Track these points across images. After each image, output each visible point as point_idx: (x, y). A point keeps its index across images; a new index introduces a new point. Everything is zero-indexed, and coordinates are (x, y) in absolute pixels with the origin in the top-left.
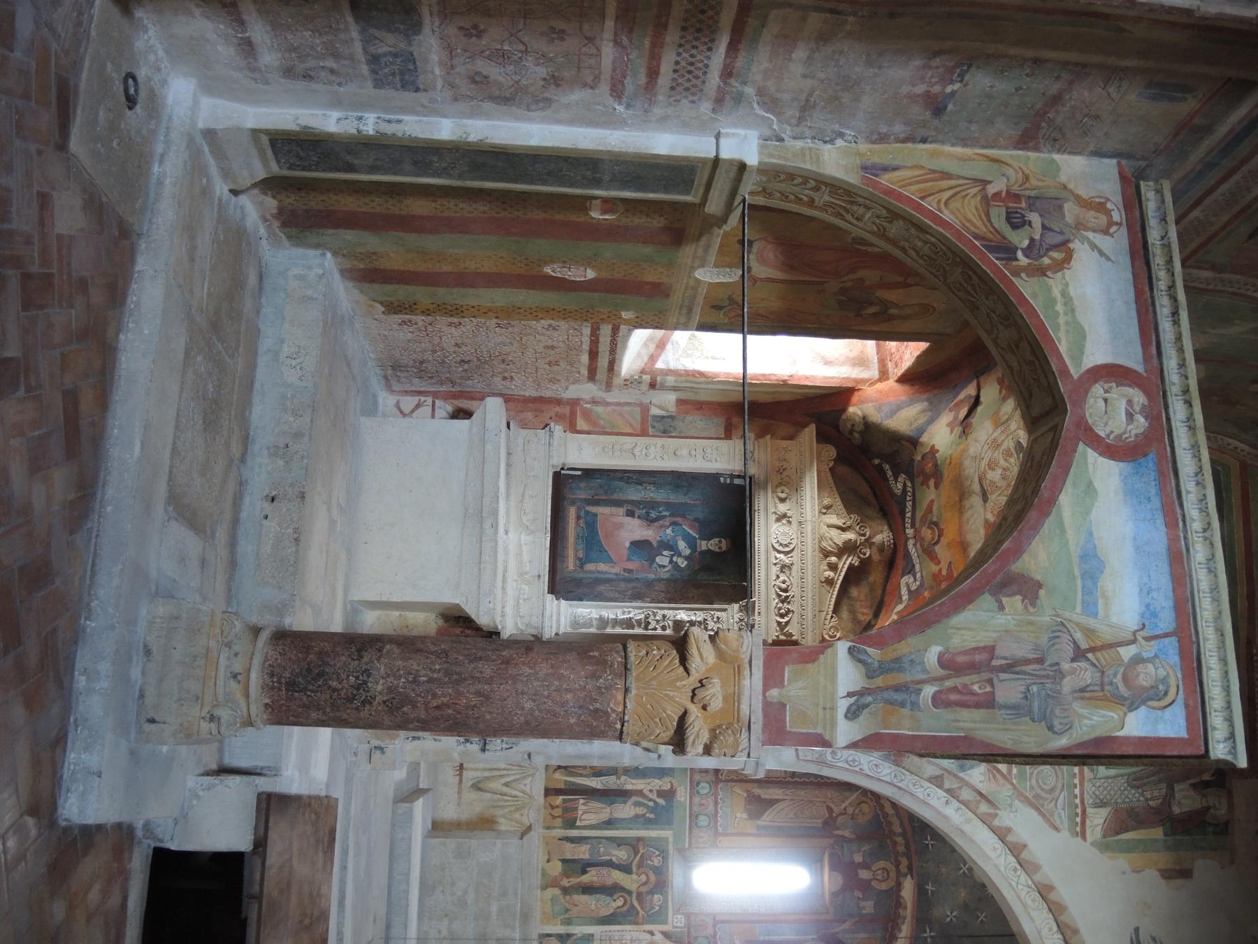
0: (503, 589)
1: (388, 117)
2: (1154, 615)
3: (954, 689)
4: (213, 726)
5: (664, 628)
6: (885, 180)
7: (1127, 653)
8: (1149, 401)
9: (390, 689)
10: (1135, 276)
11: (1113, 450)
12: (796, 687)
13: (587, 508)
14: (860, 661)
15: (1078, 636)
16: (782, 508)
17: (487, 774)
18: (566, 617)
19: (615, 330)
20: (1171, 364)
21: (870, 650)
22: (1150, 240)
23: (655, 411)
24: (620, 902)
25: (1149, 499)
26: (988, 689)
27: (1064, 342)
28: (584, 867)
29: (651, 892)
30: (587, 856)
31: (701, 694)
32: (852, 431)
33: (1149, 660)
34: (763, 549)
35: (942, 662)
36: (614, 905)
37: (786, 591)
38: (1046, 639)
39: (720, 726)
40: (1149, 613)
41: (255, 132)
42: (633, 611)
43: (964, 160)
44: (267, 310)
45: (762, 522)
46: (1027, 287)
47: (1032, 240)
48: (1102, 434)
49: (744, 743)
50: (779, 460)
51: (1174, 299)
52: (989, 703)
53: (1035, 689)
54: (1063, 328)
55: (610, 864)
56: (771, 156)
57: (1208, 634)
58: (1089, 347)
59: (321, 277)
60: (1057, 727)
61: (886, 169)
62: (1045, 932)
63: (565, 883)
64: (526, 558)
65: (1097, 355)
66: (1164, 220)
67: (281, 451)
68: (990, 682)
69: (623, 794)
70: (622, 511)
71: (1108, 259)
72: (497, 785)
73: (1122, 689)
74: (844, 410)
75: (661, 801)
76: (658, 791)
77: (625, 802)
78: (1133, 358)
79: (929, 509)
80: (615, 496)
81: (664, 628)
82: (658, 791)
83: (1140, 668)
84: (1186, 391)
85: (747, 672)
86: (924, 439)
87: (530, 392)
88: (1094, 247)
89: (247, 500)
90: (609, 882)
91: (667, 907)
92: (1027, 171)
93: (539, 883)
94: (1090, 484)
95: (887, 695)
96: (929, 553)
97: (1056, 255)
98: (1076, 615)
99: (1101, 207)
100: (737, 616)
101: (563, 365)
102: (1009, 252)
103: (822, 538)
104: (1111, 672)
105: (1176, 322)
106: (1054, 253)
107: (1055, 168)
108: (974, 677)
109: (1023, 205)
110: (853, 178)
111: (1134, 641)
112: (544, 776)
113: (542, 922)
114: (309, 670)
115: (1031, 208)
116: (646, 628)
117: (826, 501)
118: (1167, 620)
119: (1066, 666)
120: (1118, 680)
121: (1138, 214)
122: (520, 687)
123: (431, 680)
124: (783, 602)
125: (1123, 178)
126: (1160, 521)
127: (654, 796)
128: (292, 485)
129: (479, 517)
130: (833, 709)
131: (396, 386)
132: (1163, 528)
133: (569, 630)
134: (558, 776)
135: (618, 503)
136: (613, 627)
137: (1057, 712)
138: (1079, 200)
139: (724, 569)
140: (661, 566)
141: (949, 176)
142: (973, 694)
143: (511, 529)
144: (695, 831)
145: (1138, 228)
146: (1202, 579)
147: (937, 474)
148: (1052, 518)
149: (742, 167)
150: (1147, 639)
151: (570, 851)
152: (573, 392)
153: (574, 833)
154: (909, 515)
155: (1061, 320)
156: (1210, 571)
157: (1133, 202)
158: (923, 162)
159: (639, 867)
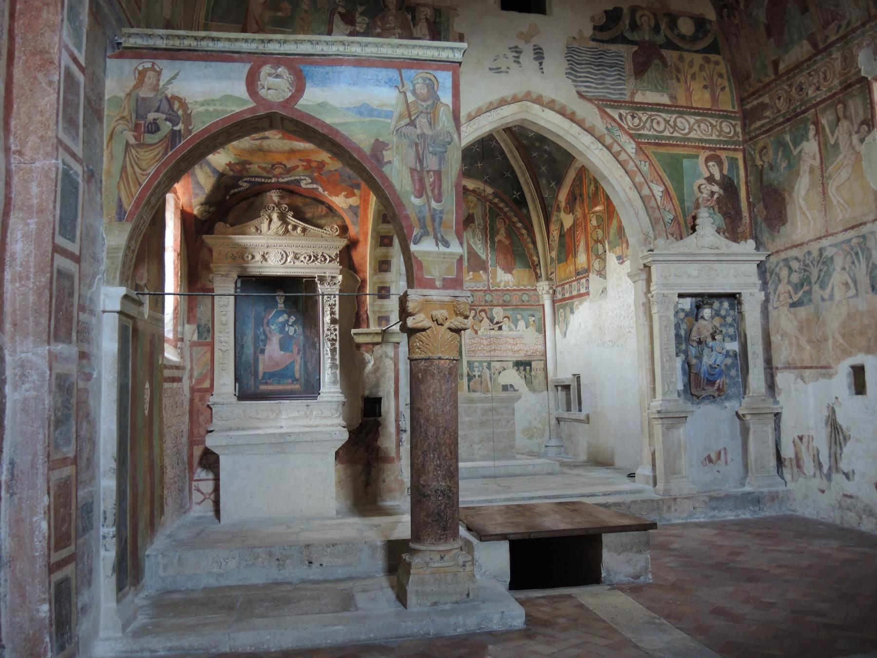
0: (316, 426)
1: (102, 520)
2: (390, 80)
3: (433, 190)
4: (467, 564)
5: (335, 330)
6: (128, 207)
7: (411, 98)
8: (268, 63)
9: (444, 478)
10: (189, 59)
11: (299, 90)
12: (435, 272)
13: (260, 378)
14: (420, 239)
15: (403, 123)
16: (258, 257)
18: (331, 388)
19: (166, 367)
20: (245, 47)
21: (415, 233)
22: (164, 46)
23: (195, 338)
25: (327, 73)
26: (432, 173)
27: (233, 108)
31: (440, 321)
32: (209, 212)
33: (414, 86)
34: (285, 270)
35: (419, 196)
37: (310, 257)
38: (406, 141)
39: (455, 311)
40: (389, 82)
41: (119, 601)
42: (326, 349)
43: (112, 157)
44: (190, 585)
45: (267, 270)
46: (198, 127)
47: (166, 119)
48: (290, 94)
49: (464, 299)
50: (226, 258)
51: (203, 38)
52: (438, 174)
53: (431, 149)
54: (224, 108)
56: (114, 278)
57: (399, 52)
58: (236, 94)
59: (164, 555)
60: (448, 139)
61: (120, 206)
62: (490, 119)
64: (296, 414)
65: (240, 90)
66: (150, 36)
67: (280, 562)
68: (428, 172)
70: (261, 357)
71: (177, 74)
73: (430, 102)
74: (195, 216)
78: (243, 69)
79: (264, 169)
80: (252, 361)
81: (335, 330)
83: (418, 92)
84: (263, 41)
85: (429, 298)
86: (220, 170)
87: (186, 419)
88: (169, 82)
89: (311, 577)
92: (118, 117)
94: (319, 105)
95: (437, 226)
96: (289, 171)
97: (176, 106)
98: (392, 122)
99: (142, 74)
100: (326, 286)
101: (177, 399)
102: (175, 136)
103: (277, 234)
104: (421, 108)
105: (219, 39)
106: (174, 107)
107: (114, 100)
108: (426, 180)
109: (142, 122)
110: (128, 227)
111: (405, 93)
114: (437, 521)
115: (144, 117)
116: (335, 340)
117: (253, 230)
118: (393, 73)
119: (419, 131)
120: (425, 104)
121: (145, 51)
122: (440, 413)
123: (439, 458)
124: (317, 259)
125: (120, 56)
126: (339, 68)
128: (301, 553)
129: (282, 444)
130: (444, 254)
131: (188, 506)
132: (343, 67)
133: (338, 386)
135: (256, 360)
136: (336, 360)
137: (442, 138)
138: (136, 87)
139: (295, 293)
140: (295, 332)
141: (124, 168)
142: (434, 181)
143: (279, 424)
145: (155, 52)
146: (370, 51)
147: (244, 163)
148: (339, 128)
149: (126, 297)
150: (403, 86)
152: (187, 391)
154: (263, 180)
155: (219, 108)
156: (366, 46)
157: (136, 53)
158: (115, 183)
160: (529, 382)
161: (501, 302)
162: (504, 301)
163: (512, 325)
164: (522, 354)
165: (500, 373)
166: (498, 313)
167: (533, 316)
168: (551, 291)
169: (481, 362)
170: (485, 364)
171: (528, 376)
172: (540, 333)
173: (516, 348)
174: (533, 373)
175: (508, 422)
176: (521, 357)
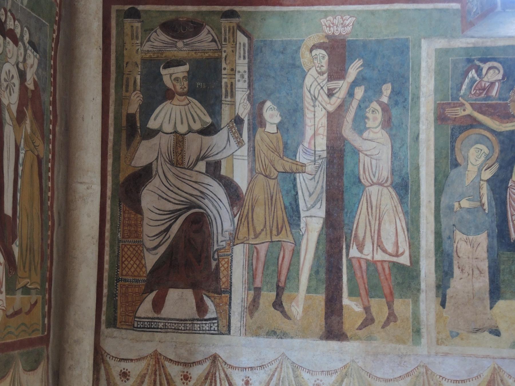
30: (483, 239)
69: (338, 157)
75: (353, 71)
76: (331, 78)
77: (356, 152)
82: (331, 78)
112: (297, 342)
127: (342, 87)
153: (427, 268)
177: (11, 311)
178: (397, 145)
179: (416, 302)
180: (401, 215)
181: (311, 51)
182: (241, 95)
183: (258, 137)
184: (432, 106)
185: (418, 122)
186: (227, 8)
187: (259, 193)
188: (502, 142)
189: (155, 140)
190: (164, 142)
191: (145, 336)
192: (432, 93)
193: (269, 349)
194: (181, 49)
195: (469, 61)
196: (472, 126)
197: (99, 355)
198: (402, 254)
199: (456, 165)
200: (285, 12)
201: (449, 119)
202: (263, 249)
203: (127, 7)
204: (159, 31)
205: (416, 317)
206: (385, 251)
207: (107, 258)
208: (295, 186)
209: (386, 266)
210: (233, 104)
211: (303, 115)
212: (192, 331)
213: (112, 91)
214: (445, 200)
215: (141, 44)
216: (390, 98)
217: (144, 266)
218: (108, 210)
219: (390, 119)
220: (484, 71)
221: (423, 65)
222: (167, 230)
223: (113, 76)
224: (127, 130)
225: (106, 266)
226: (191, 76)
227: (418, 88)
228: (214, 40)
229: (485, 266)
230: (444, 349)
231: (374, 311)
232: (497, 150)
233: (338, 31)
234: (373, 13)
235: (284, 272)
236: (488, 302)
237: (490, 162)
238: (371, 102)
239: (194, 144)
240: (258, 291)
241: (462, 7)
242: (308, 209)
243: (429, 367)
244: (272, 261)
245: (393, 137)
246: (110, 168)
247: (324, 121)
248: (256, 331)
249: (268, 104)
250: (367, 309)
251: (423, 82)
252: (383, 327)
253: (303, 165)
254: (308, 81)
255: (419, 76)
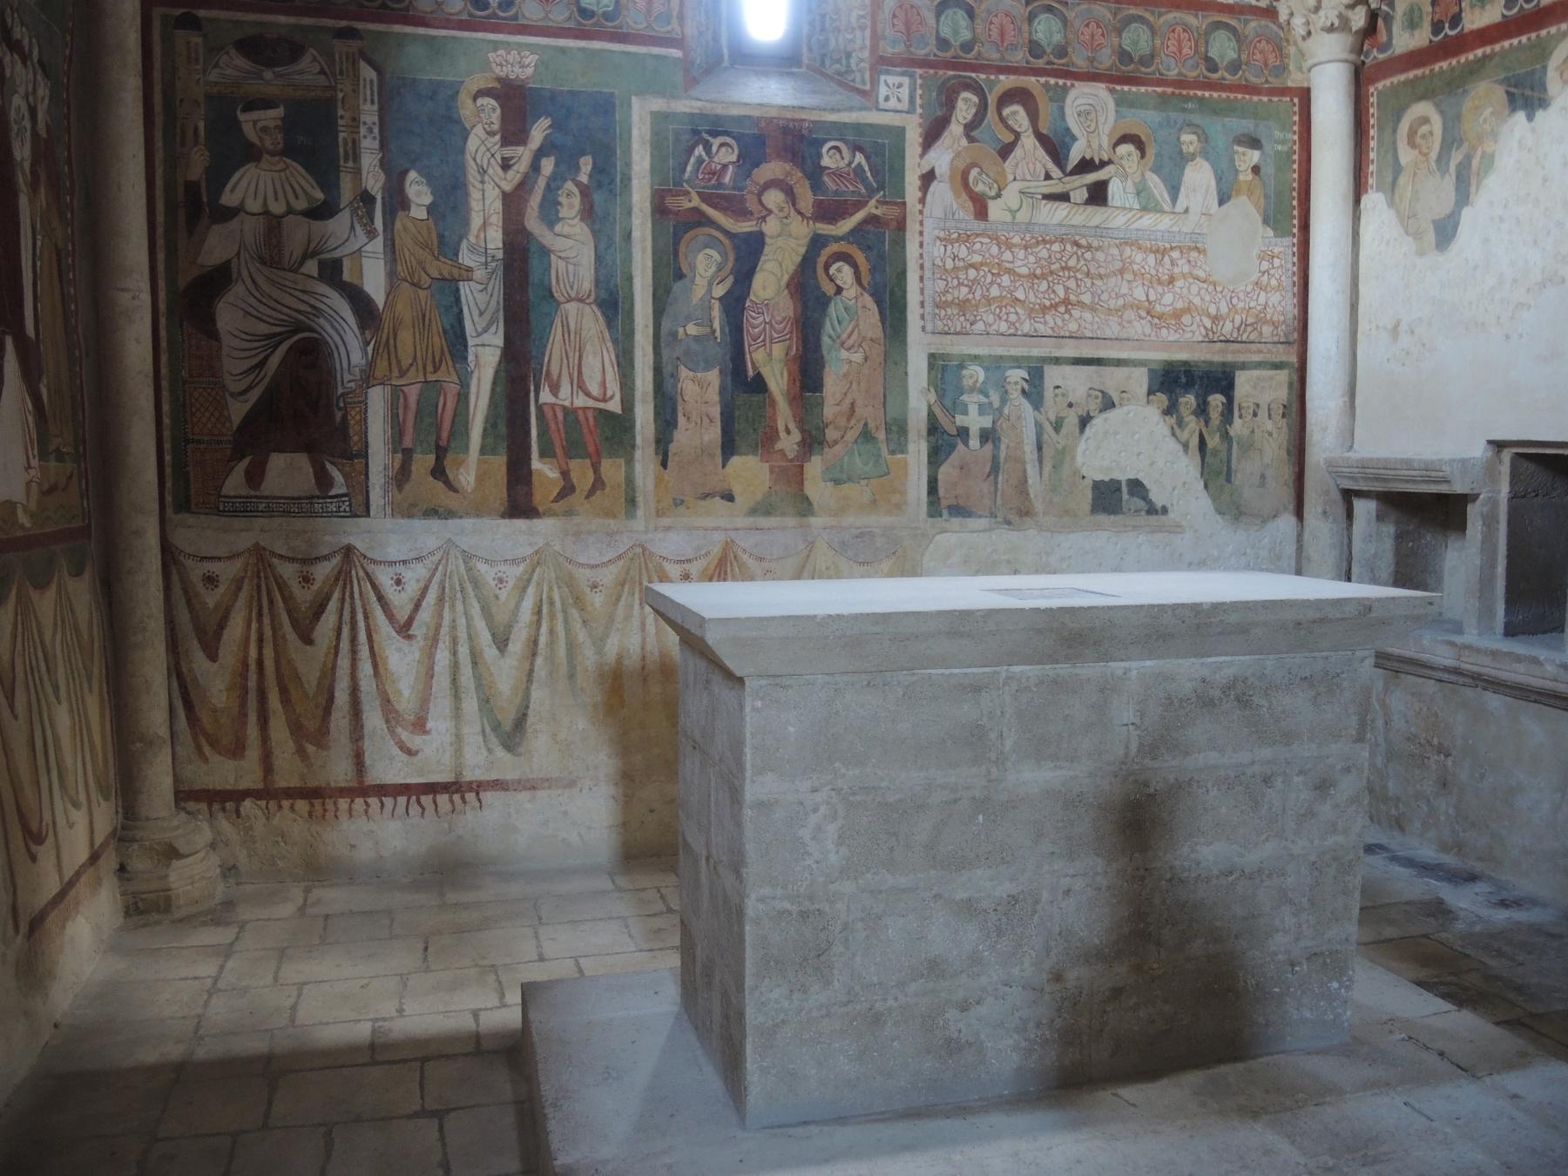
17: (470, 705)
24: (844, 274)
28: (744, 385)
29: (815, 175)
30: (713, 377)
36: (851, 290)
55: (735, 304)
63: (789, 442)
69: (520, 261)
72: (505, 671)
75: (538, 132)
77: (545, 252)
82: (506, 141)
90: (786, 307)
91: (858, 128)
93: (791, 521)
112: (468, 523)
113: (899, 507)
127: (523, 155)
134: (467, 476)
144: (633, 20)
151: (699, 430)
159: (742, 213)
160: (1216, 471)
161: (1106, 59)
162: (1124, 56)
163: (1156, 184)
164: (1194, 330)
165: (1084, 421)
166: (1091, 113)
167: (1255, 143)
168: (1359, 19)
169: (995, 365)
170: (1017, 375)
171: (1213, 442)
172: (1280, 231)
173: (1168, 301)
174: (1238, 427)
175: (1323, 787)
176: (1185, 344)
177: (46, 486)
178: (602, 246)
179: (630, 462)
180: (609, 344)
181: (475, 99)
182: (370, 160)
183: (398, 225)
184: (648, 192)
185: (629, 213)
186: (343, 23)
187: (404, 311)
188: (736, 248)
189: (234, 224)
190: (248, 229)
191: (238, 523)
192: (648, 174)
193: (428, 534)
194: (270, 81)
195: (695, 132)
196: (699, 224)
197: (168, 552)
198: (612, 397)
199: (680, 276)
200: (434, 38)
201: (670, 212)
202: (413, 393)
203: (181, 11)
204: (233, 52)
205: (630, 481)
206: (588, 394)
207: (166, 408)
208: (458, 300)
209: (590, 414)
210: (357, 172)
211: (467, 195)
212: (312, 515)
213: (159, 144)
214: (666, 325)
215: (205, 70)
216: (590, 176)
217: (229, 419)
218: (163, 333)
219: (592, 206)
220: (714, 149)
221: (635, 133)
222: (262, 364)
223: (159, 120)
224: (187, 208)
225: (166, 421)
226: (288, 126)
227: (628, 165)
228: (322, 72)
229: (716, 411)
230: (666, 521)
231: (574, 476)
232: (731, 257)
233: (515, 73)
234: (563, 50)
235: (447, 424)
236: (719, 460)
237: (723, 274)
238: (565, 180)
239: (297, 233)
240: (408, 454)
241: (685, 56)
242: (479, 335)
243: (648, 546)
244: (428, 410)
245: (596, 234)
246: (161, 267)
247: (498, 205)
248: (408, 510)
249: (413, 175)
250: (565, 474)
251: (636, 157)
252: (587, 497)
253: (469, 270)
254: (472, 143)
255: (629, 148)
